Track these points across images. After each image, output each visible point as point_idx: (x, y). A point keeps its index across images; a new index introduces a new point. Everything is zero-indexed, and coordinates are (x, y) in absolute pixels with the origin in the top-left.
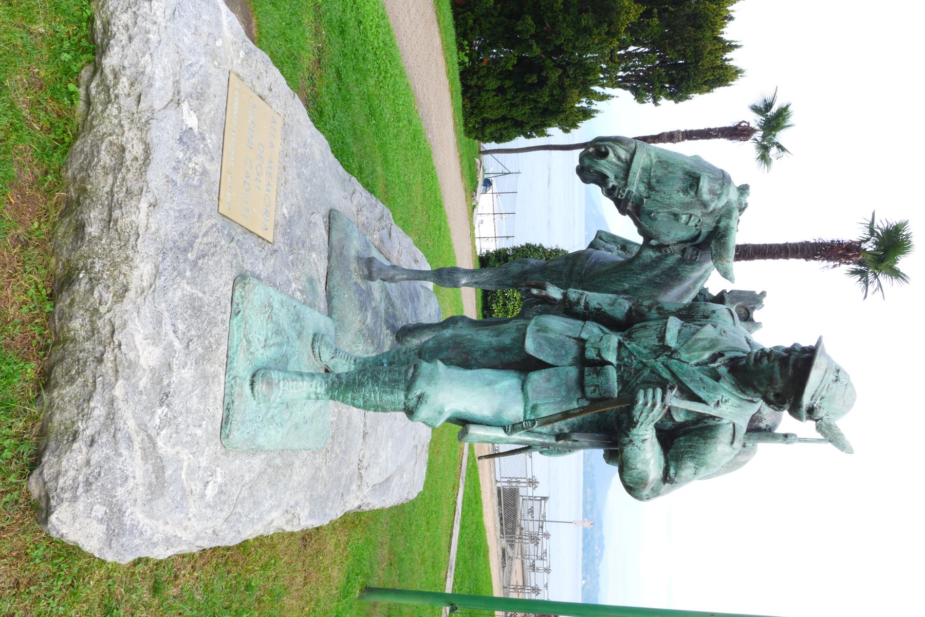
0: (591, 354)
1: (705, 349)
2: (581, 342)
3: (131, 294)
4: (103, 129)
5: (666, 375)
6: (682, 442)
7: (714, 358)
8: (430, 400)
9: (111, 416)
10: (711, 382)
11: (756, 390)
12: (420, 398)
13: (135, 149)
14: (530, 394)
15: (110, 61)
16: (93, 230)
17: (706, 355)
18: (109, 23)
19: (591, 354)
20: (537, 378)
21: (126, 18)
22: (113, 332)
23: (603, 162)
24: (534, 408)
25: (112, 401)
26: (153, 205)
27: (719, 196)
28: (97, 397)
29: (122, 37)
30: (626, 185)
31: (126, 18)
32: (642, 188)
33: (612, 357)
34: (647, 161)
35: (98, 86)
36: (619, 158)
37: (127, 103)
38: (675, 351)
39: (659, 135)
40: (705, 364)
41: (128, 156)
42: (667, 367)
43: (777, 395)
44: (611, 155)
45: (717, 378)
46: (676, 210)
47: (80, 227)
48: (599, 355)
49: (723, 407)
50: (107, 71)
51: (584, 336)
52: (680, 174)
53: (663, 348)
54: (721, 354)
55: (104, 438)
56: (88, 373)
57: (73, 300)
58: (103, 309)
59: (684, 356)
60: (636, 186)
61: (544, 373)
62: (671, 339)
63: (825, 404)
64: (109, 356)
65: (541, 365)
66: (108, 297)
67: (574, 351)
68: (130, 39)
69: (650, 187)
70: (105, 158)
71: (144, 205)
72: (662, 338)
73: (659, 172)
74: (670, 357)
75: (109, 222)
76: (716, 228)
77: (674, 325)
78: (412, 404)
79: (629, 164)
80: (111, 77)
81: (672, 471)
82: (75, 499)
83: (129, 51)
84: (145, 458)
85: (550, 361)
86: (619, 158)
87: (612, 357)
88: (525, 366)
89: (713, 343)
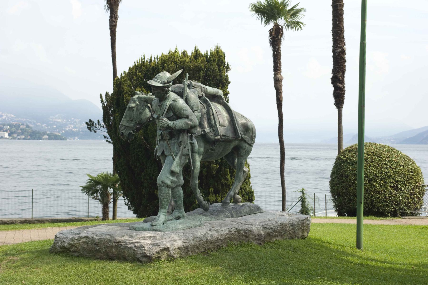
2: (160, 140)
6: (177, 114)
7: (159, 106)
8: (163, 180)
9: (133, 243)
11: (164, 96)
12: (163, 182)
13: (85, 240)
16: (97, 248)
17: (158, 107)
18: (60, 247)
21: (60, 243)
22: (116, 242)
23: (125, 134)
25: (130, 243)
26: (96, 236)
29: (63, 244)
30: (132, 127)
32: (133, 123)
34: (125, 121)
36: (124, 129)
37: (76, 241)
39: (276, 89)
43: (163, 91)
44: (123, 131)
45: (162, 105)
46: (139, 113)
47: (97, 251)
49: (167, 104)
52: (129, 112)
55: (136, 244)
60: (132, 124)
63: (163, 80)
64: (121, 244)
65: (163, 151)
66: (110, 243)
67: (162, 142)
68: (64, 242)
69: (132, 120)
70: (85, 246)
71: (95, 237)
73: (128, 118)
75: (97, 244)
76: (145, 101)
78: (165, 185)
79: (126, 127)
81: (185, 116)
82: (145, 250)
84: (146, 240)
86: (124, 129)
89: (156, 106)
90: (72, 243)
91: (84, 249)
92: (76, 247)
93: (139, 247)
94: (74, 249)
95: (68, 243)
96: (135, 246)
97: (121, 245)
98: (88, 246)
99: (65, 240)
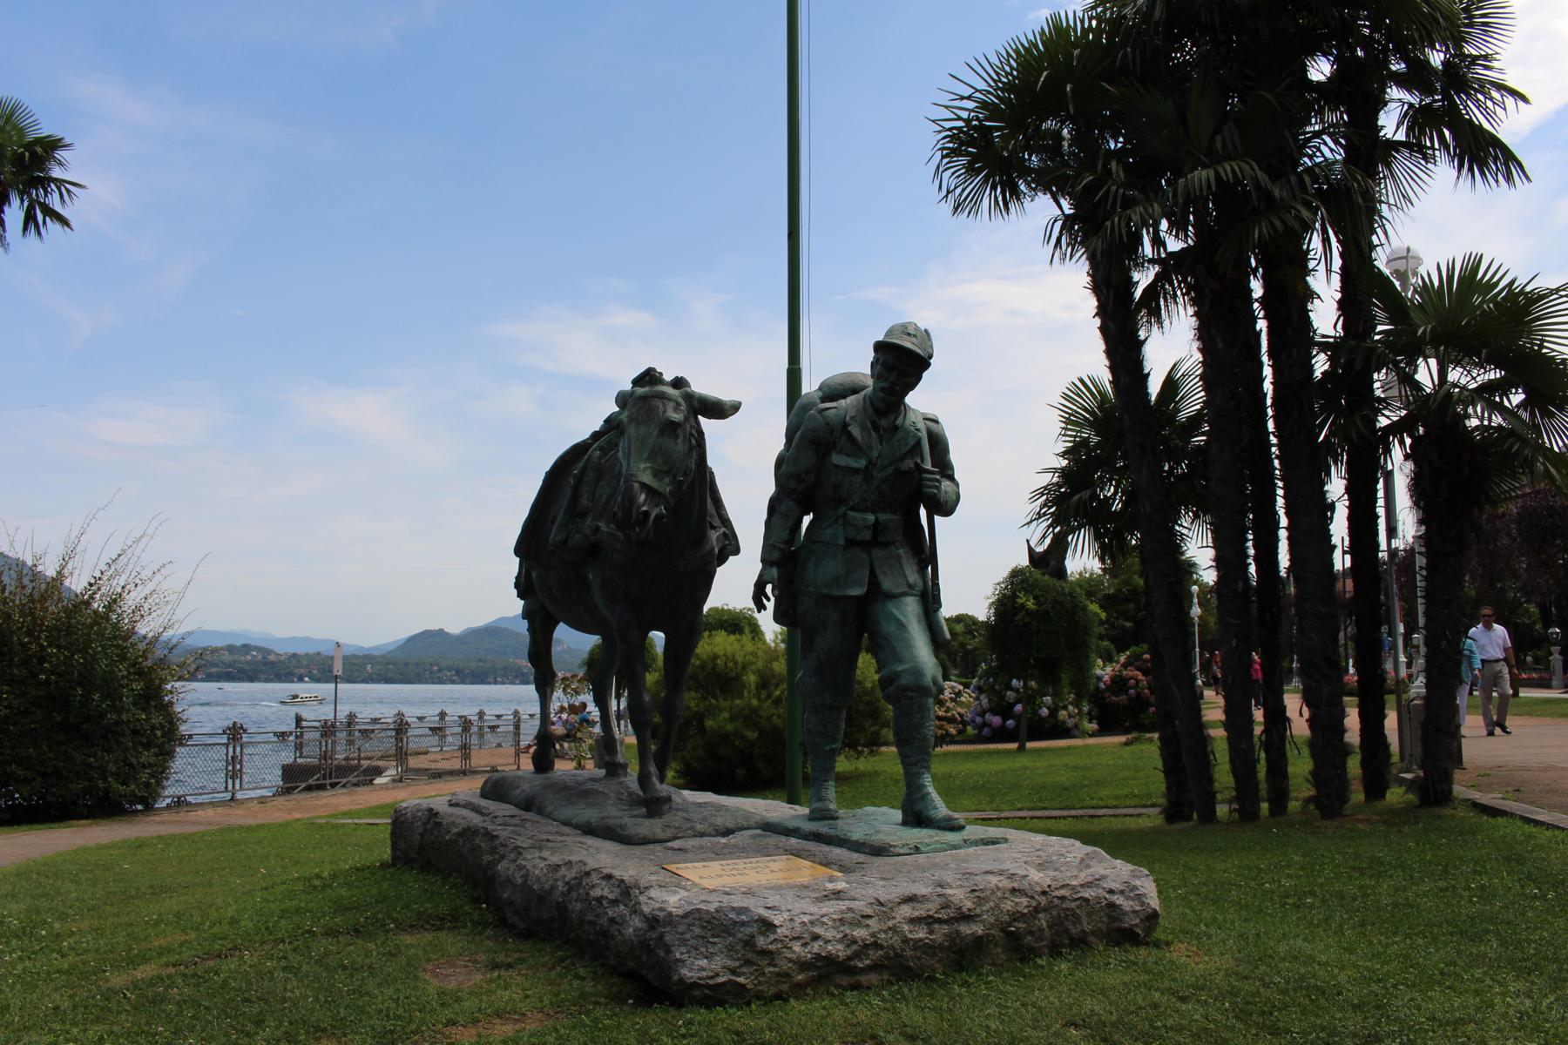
0: (868, 535)
1: (870, 436)
3: (1015, 885)
4: (896, 941)
5: (890, 470)
10: (900, 435)
13: (906, 911)
14: (901, 590)
15: (839, 950)
19: (868, 535)
20: (887, 584)
21: (797, 947)
24: (911, 587)
27: (678, 404)
28: (1086, 895)
29: (816, 947)
31: (797, 947)
32: (667, 480)
33: (871, 518)
35: (861, 960)
38: (870, 461)
40: (881, 438)
41: (917, 914)
42: (883, 469)
48: (867, 527)
50: (849, 953)
51: (841, 542)
53: (866, 473)
54: (873, 423)
56: (1073, 905)
57: (1031, 933)
58: (1034, 904)
59: (875, 454)
61: (881, 578)
62: (861, 463)
64: (1057, 893)
68: (816, 937)
70: (921, 934)
72: (856, 471)
74: (874, 466)
77: (838, 459)
80: (855, 947)
83: (829, 935)
85: (867, 573)
87: (871, 518)
88: (876, 593)
89: (863, 427)
90: (860, 933)
91: (918, 945)
92: (881, 947)
93: (1122, 892)
94: (875, 955)
95: (840, 941)
96: (1111, 892)
97: (1063, 898)
98: (931, 933)
99: (818, 930)
